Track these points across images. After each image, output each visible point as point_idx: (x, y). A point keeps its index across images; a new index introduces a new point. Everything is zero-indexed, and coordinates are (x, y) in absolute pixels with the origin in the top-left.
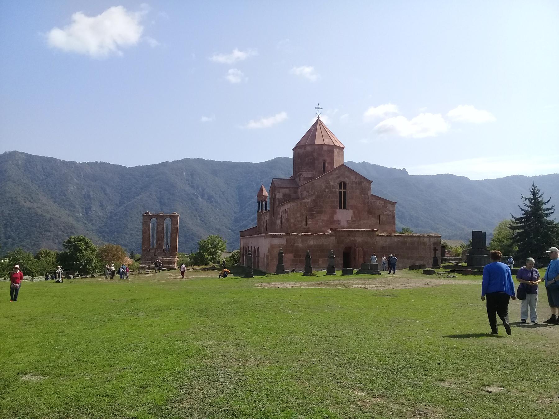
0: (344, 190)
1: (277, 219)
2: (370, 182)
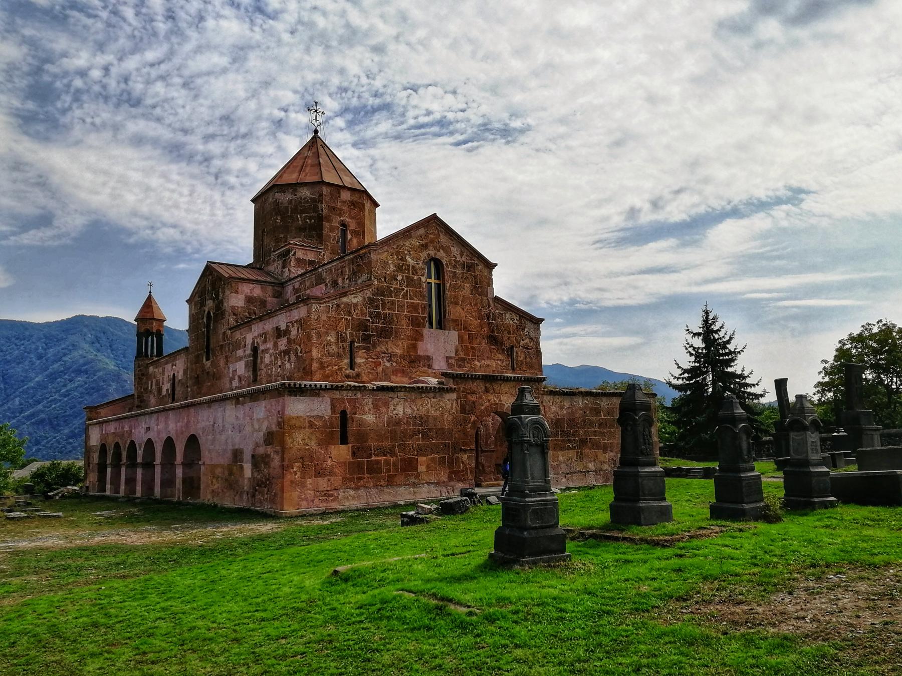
0: (437, 281)
1: (227, 361)
2: (491, 266)
